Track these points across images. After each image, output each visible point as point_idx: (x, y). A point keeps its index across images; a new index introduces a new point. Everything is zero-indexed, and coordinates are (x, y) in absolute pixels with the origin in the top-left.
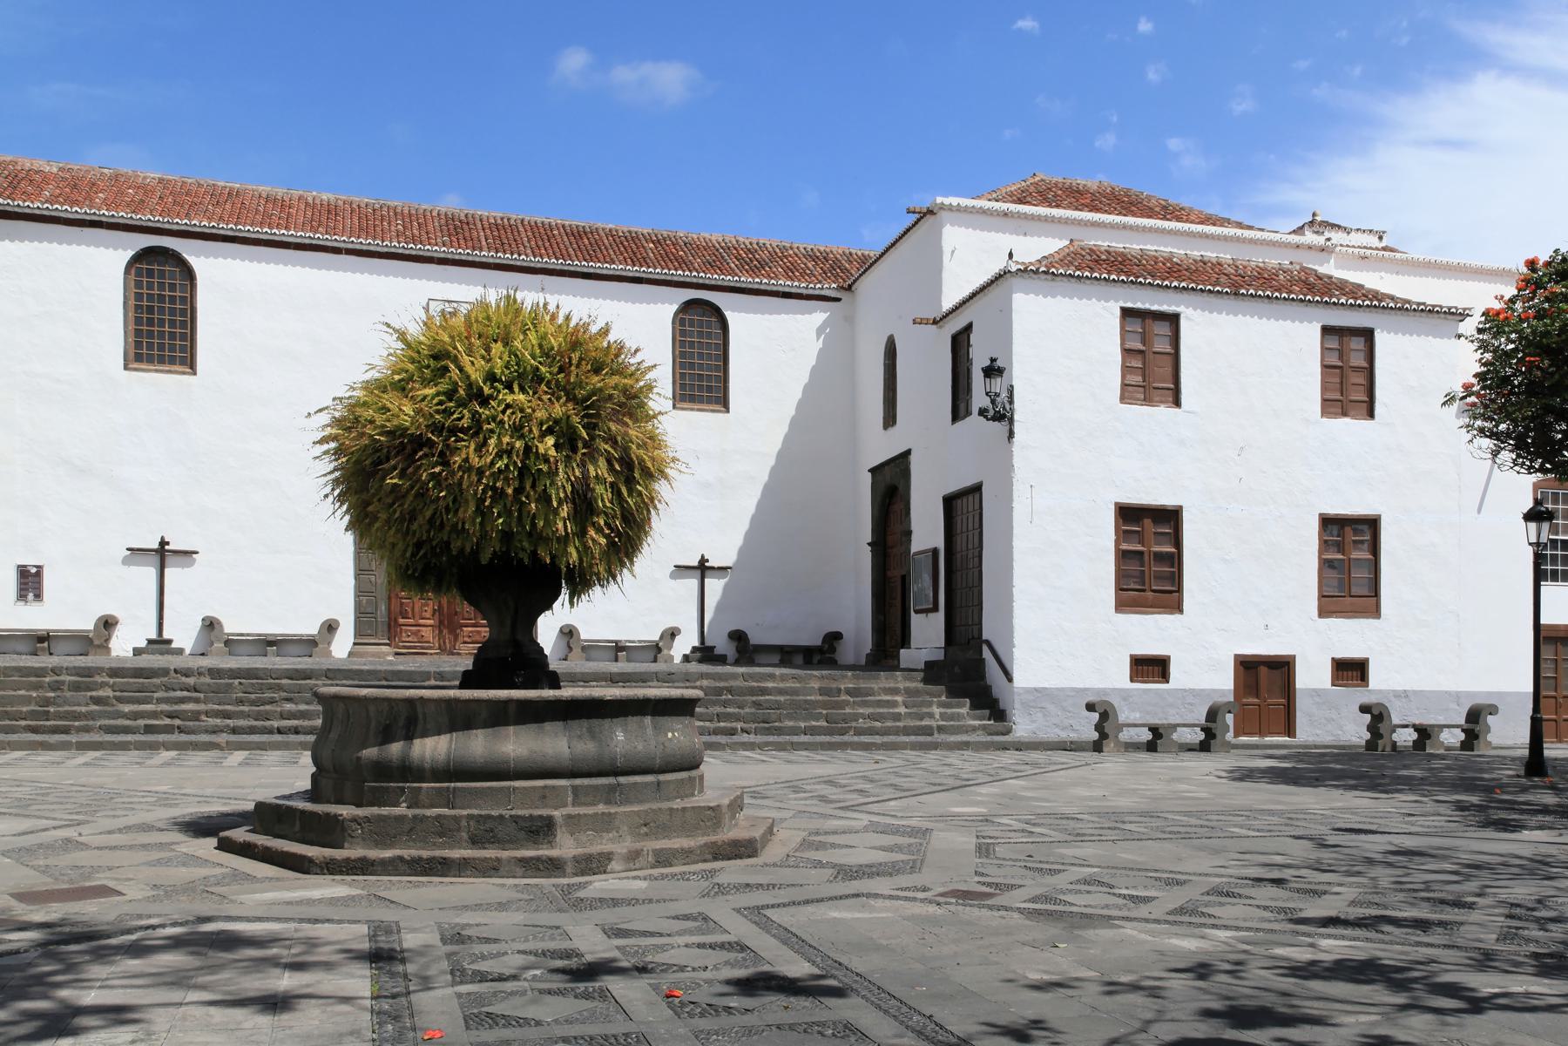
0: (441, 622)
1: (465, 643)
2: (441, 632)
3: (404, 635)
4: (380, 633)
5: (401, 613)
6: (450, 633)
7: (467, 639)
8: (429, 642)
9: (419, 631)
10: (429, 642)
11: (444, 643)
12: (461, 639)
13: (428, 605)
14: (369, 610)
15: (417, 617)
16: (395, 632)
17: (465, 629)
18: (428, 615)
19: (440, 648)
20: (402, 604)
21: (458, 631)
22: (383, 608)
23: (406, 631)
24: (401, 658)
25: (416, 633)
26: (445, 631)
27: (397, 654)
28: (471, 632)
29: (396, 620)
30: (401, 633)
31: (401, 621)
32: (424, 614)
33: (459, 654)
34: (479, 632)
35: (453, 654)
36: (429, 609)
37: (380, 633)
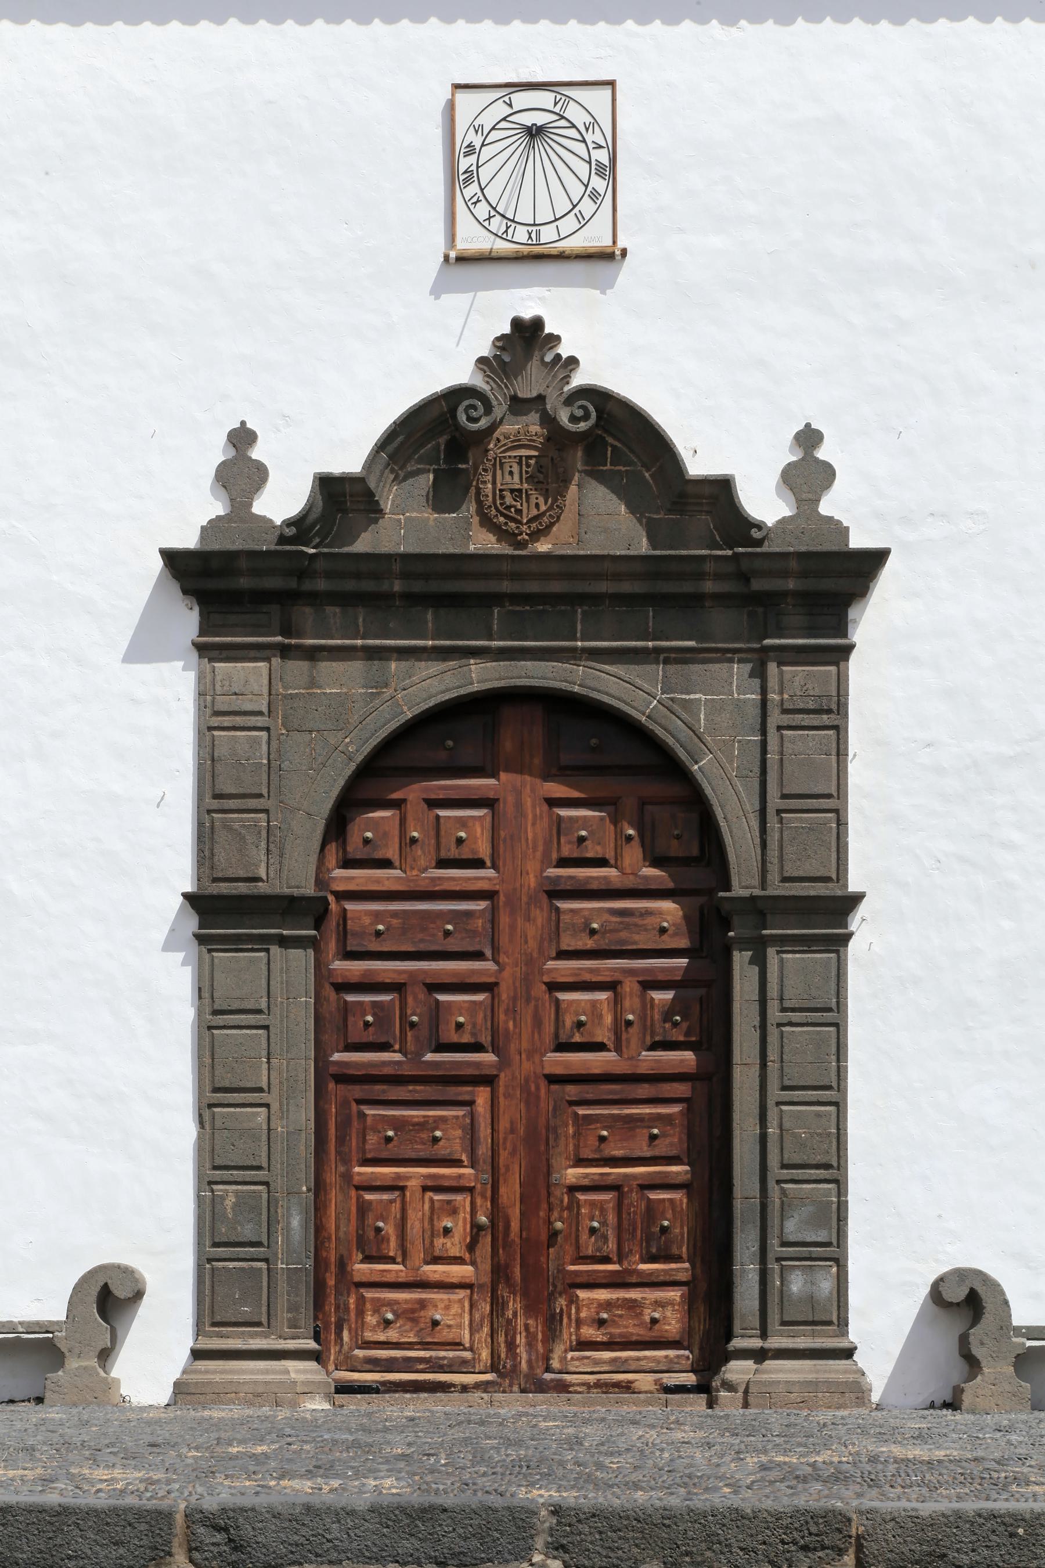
0: (499, 1272)
1: (584, 1345)
2: (498, 1306)
3: (371, 1319)
4: (283, 1315)
5: (361, 1243)
6: (530, 1309)
7: (589, 1332)
8: (457, 1345)
9: (422, 1304)
10: (457, 1345)
11: (511, 1346)
12: (568, 1333)
13: (453, 1211)
14: (247, 1231)
15: (417, 1254)
16: (342, 1308)
17: (582, 1294)
18: (454, 1246)
19: (494, 1368)
20: (363, 1209)
21: (562, 1302)
22: (296, 1222)
23: (379, 1306)
24: (354, 1403)
25: (410, 1314)
26: (514, 1305)
27: (344, 1389)
28: (608, 1305)
29: (342, 1265)
30: (361, 1313)
31: (361, 1269)
32: (439, 1242)
33: (563, 1387)
34: (633, 1306)
35: (541, 1387)
36: (459, 1225)
37: (283, 1315)
